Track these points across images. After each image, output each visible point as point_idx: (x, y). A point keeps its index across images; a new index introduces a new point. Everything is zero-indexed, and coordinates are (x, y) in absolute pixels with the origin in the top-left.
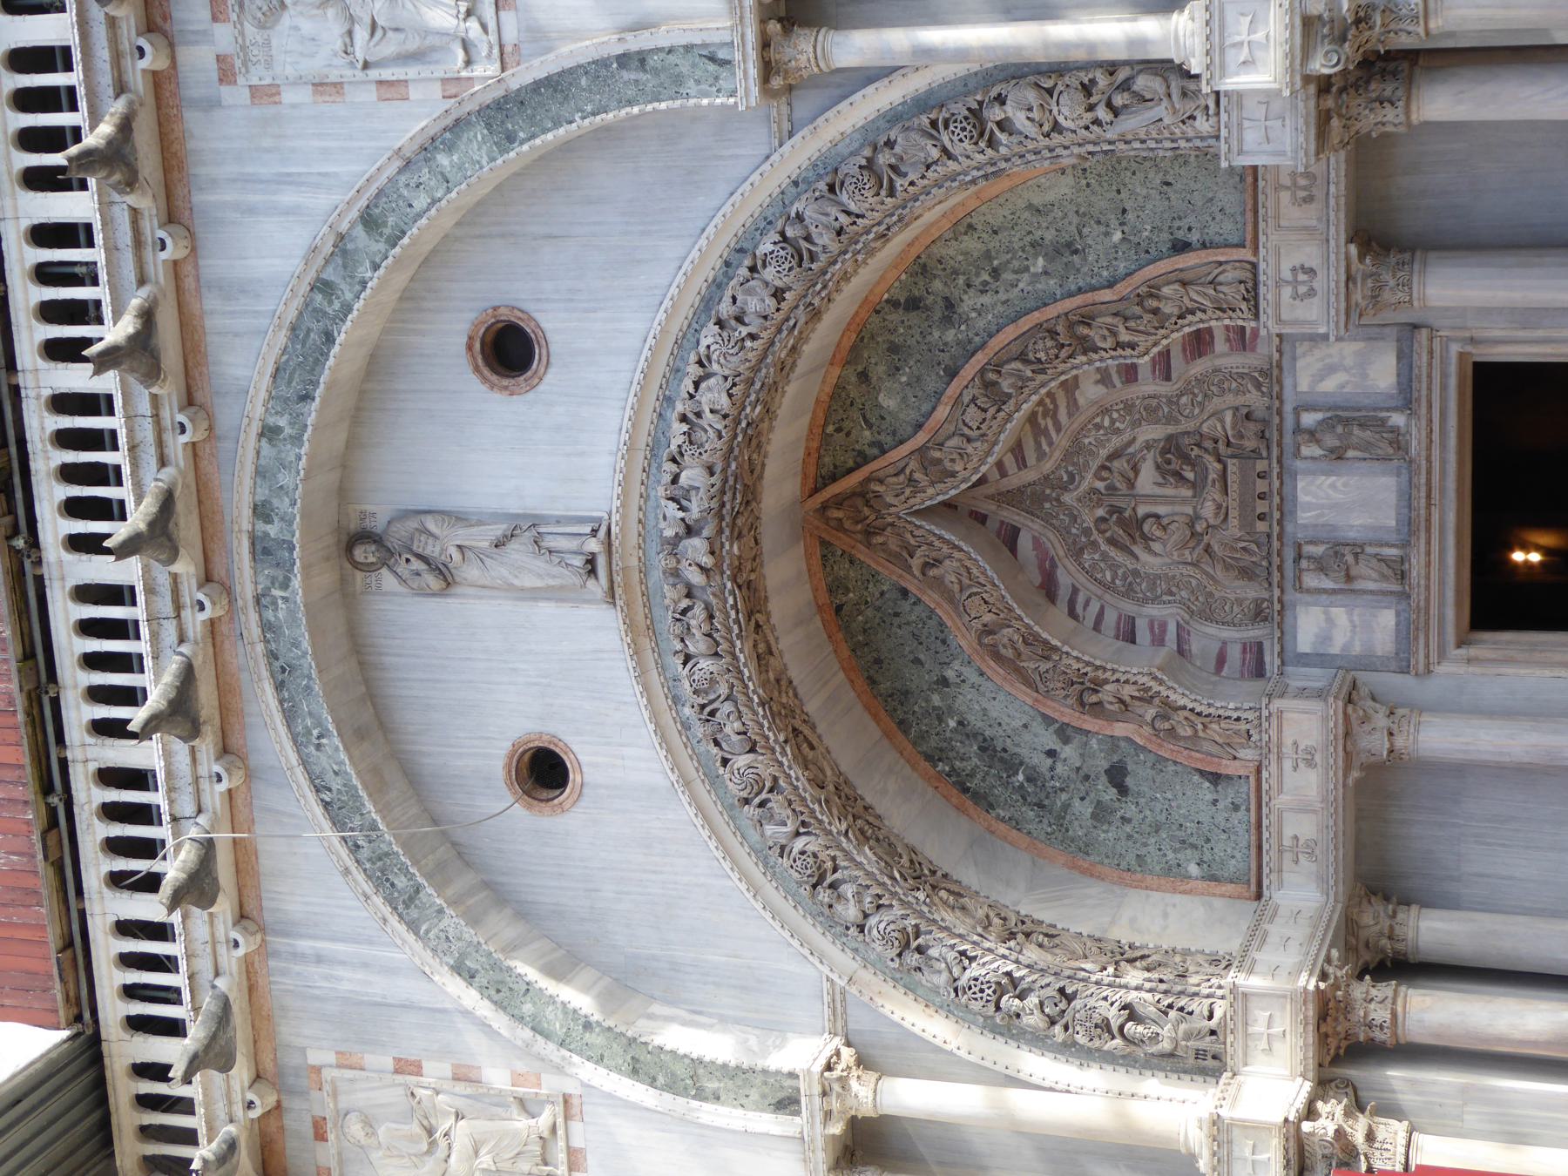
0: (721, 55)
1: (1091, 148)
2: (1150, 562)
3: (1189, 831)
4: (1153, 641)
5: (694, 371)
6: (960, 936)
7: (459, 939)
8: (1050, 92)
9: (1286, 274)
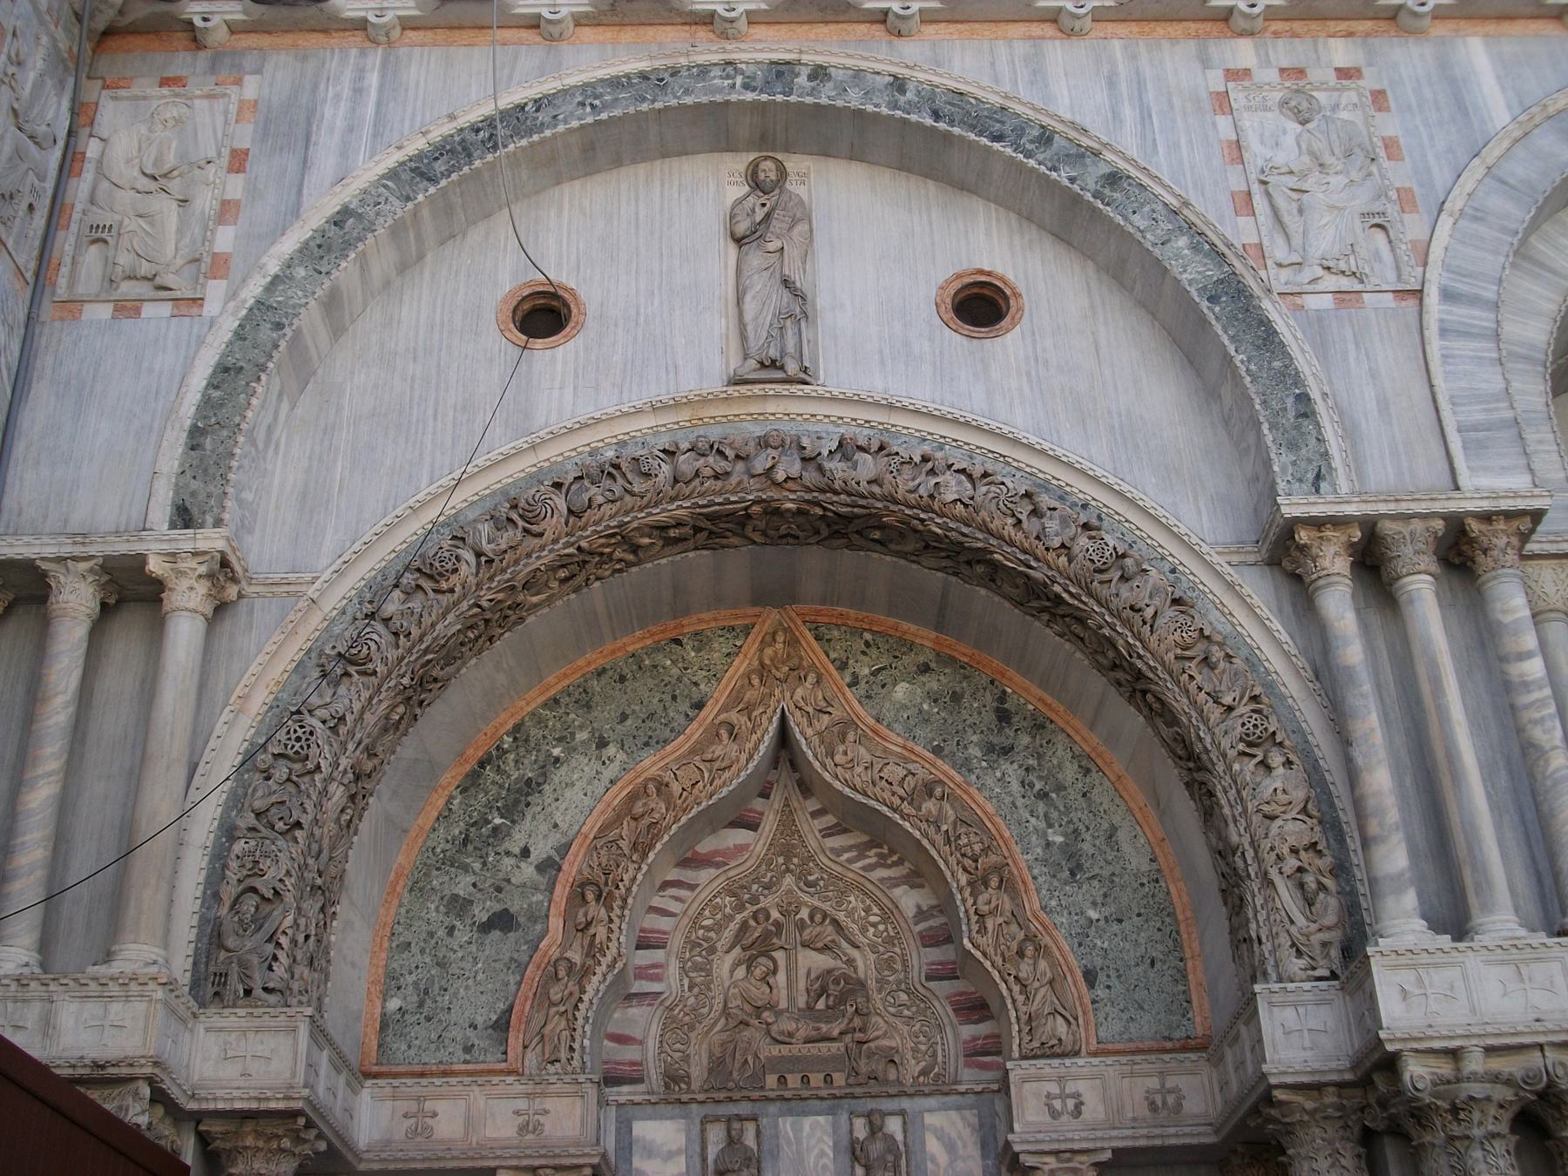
0: (1324, 486)
1: (1250, 854)
2: (724, 965)
4: (640, 968)
5: (977, 472)
7: (378, 214)
8: (1304, 810)
9: (1071, 1087)
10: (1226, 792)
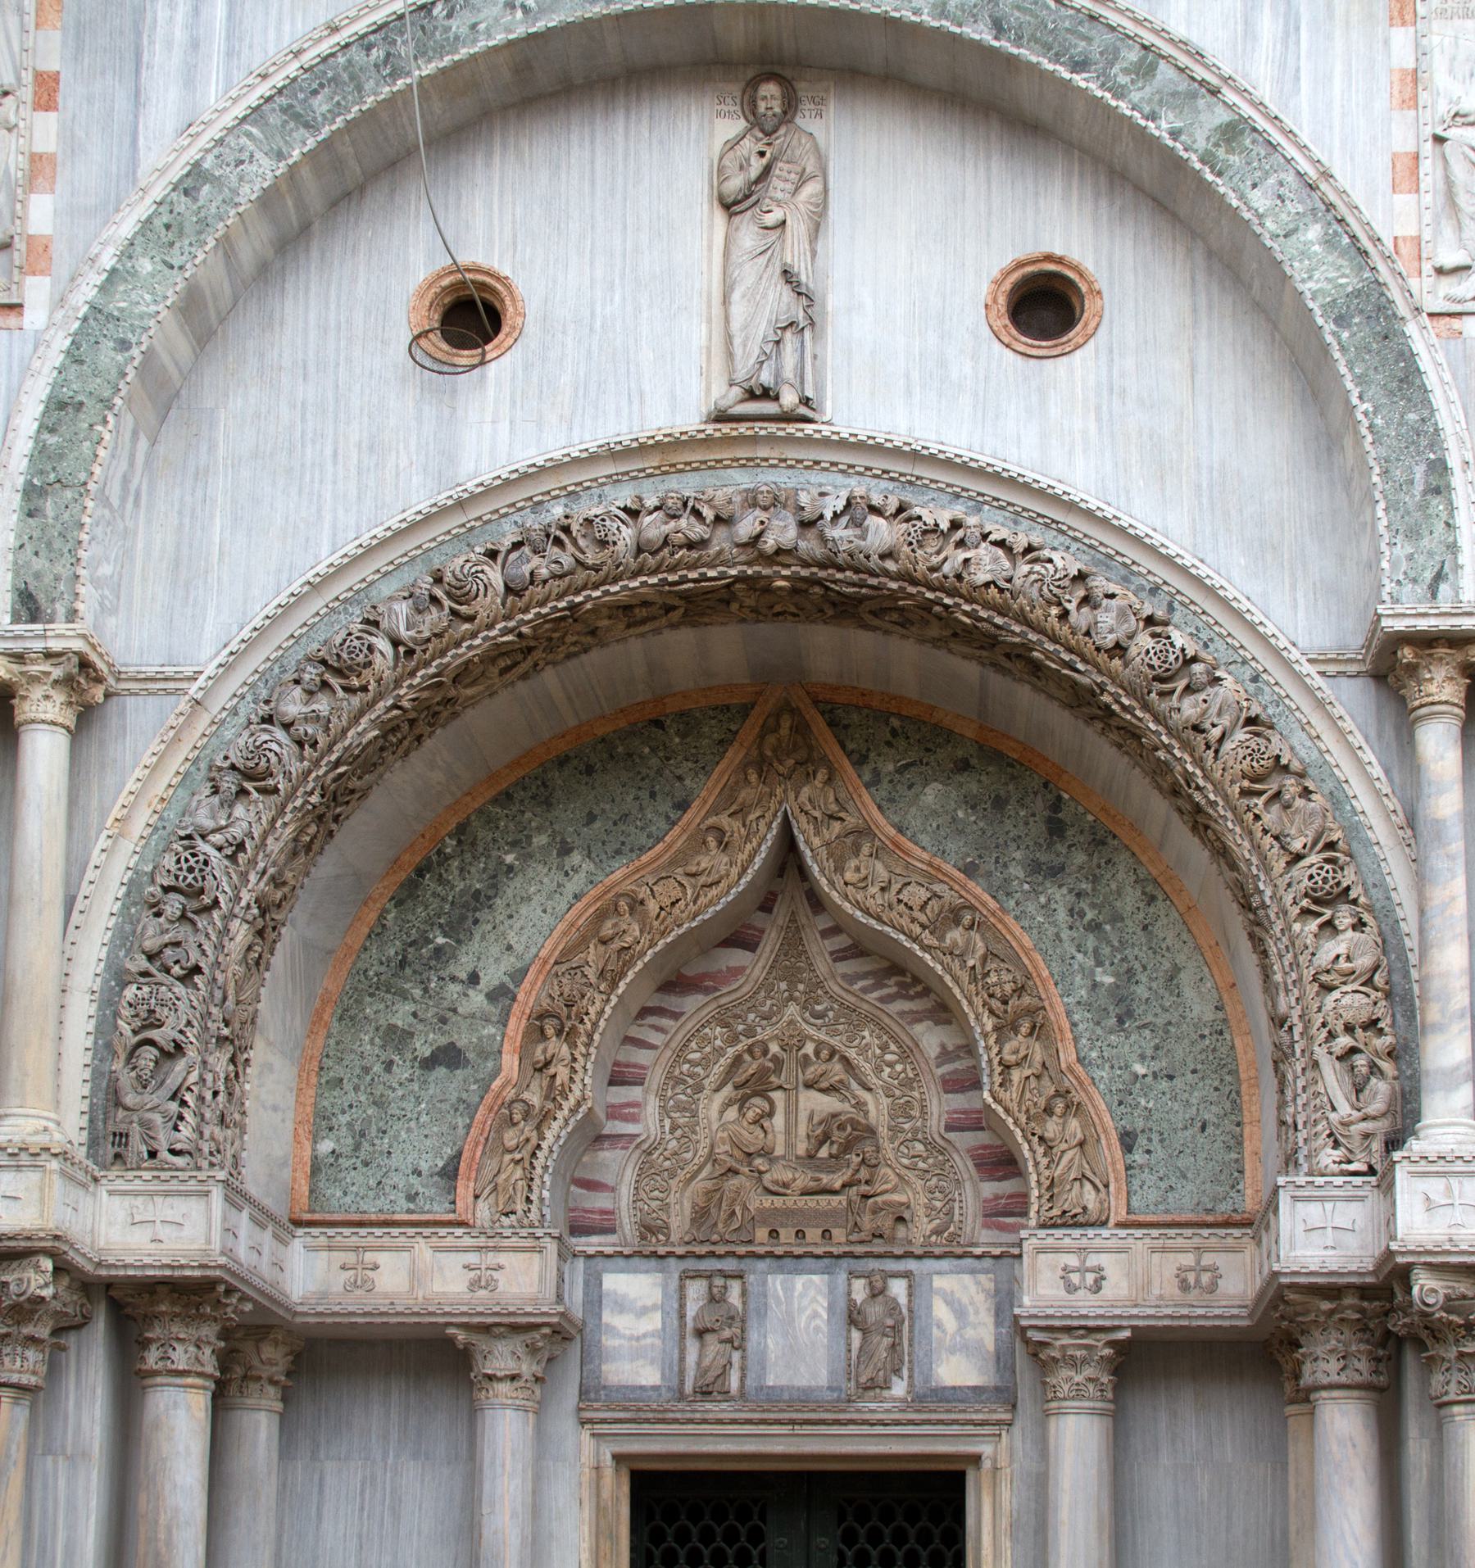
3: (377, 1142)
4: (613, 1106)
6: (263, 844)
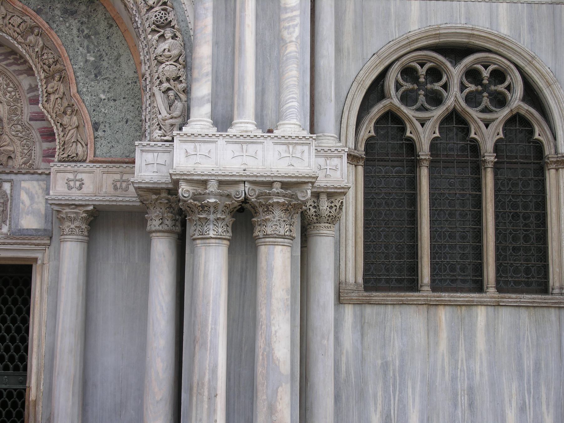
1: (148, 80)
8: (177, 61)
9: (79, 176)
10: (143, 49)
